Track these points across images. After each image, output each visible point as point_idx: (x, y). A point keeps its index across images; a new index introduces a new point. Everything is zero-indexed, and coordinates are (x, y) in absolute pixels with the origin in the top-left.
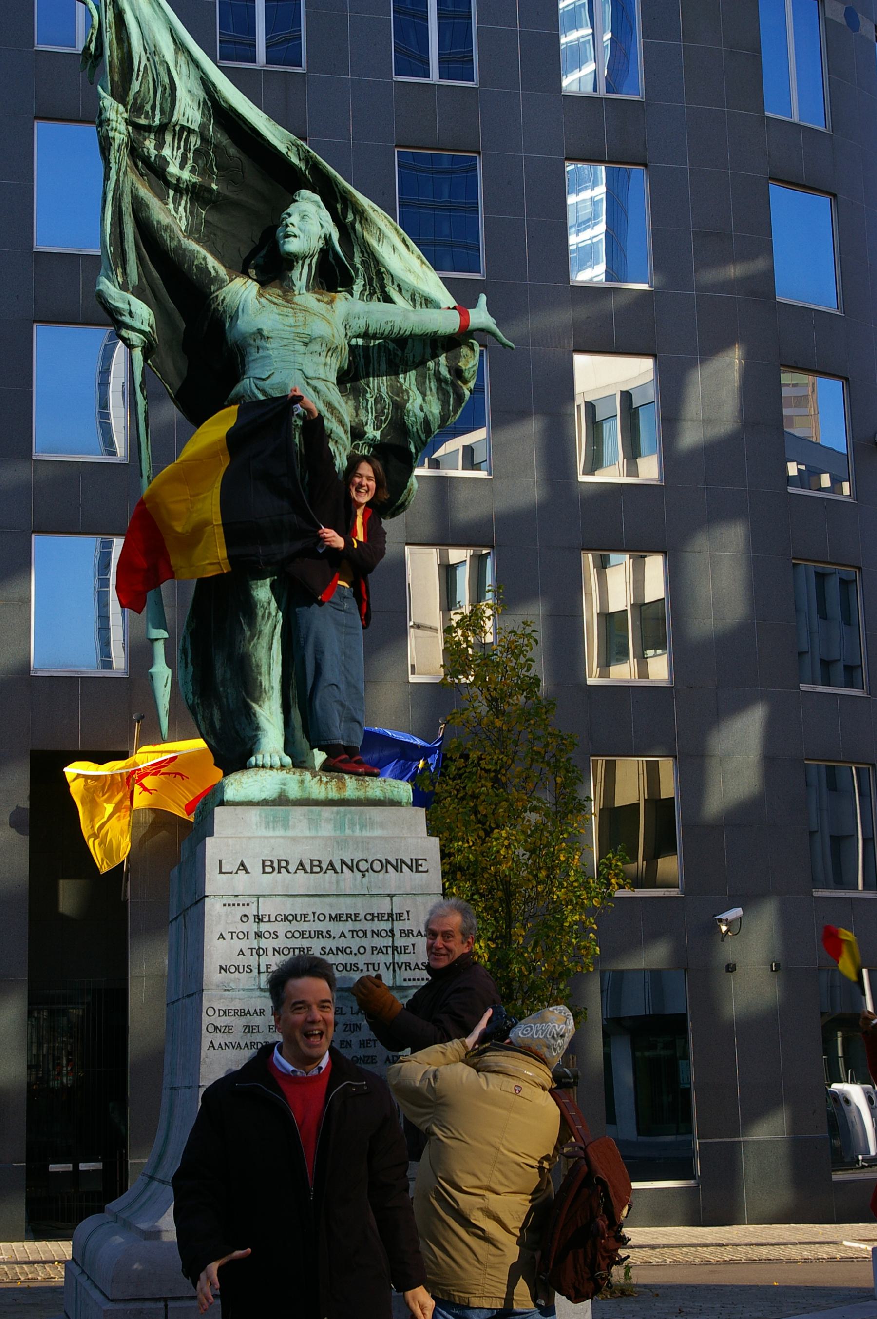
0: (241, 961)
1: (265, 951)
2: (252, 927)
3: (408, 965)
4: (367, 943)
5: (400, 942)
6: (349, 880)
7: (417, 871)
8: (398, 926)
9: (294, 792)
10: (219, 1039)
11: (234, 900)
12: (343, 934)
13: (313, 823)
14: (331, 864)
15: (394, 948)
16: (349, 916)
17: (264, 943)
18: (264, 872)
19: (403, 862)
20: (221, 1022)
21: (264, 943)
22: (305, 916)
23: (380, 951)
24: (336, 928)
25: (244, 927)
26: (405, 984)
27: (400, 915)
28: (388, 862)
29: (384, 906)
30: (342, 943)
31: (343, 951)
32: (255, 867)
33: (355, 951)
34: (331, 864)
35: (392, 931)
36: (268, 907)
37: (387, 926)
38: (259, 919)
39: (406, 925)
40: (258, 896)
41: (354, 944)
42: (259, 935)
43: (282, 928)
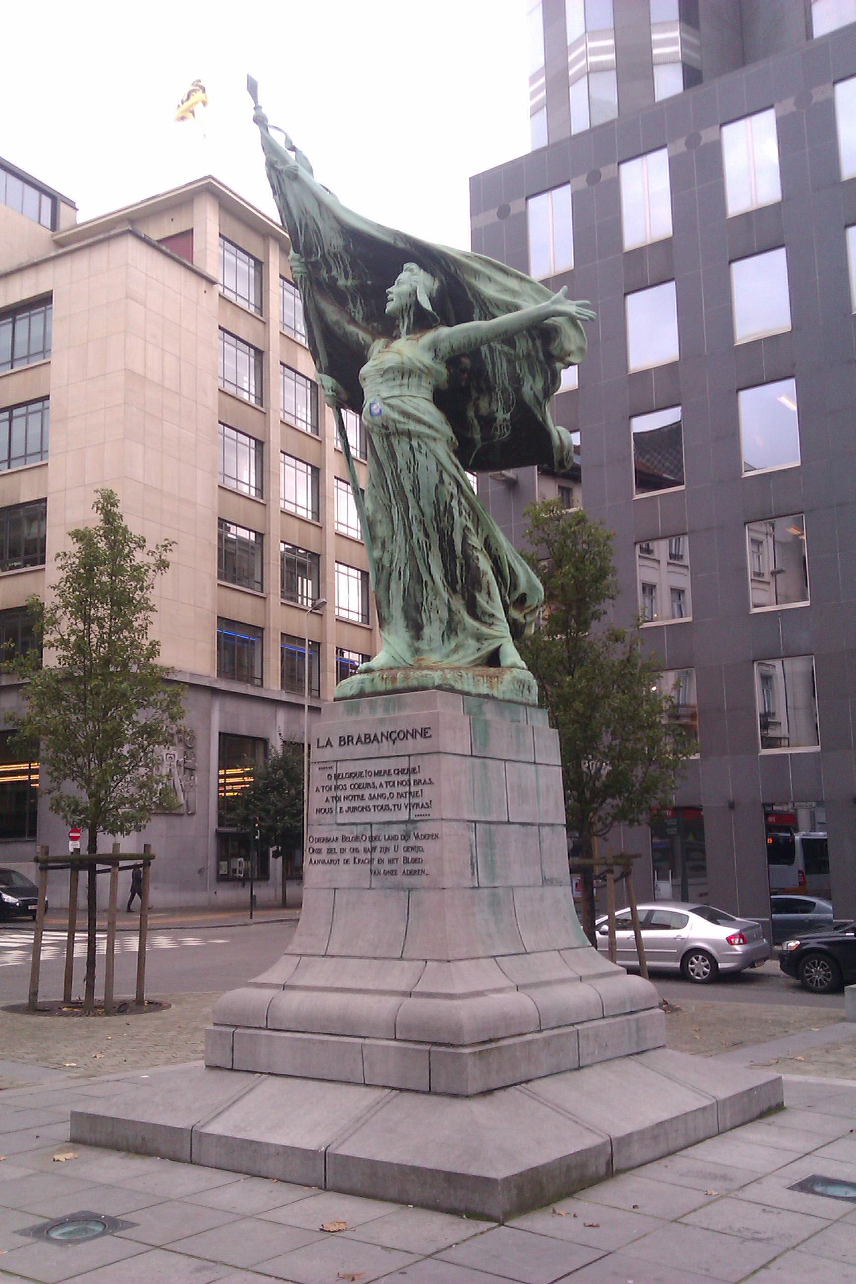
0: (327, 806)
1: (340, 799)
2: (333, 783)
3: (418, 805)
4: (395, 790)
5: (414, 789)
6: (386, 747)
7: (425, 737)
8: (413, 777)
9: (368, 688)
10: (315, 857)
11: (325, 766)
12: (381, 785)
13: (372, 708)
14: (375, 736)
15: (410, 793)
16: (385, 772)
17: (339, 793)
18: (340, 745)
19: (416, 731)
20: (316, 846)
21: (339, 793)
22: (361, 773)
23: (402, 796)
24: (378, 780)
25: (328, 783)
26: (416, 819)
27: (414, 769)
28: (408, 732)
29: (403, 763)
30: (380, 791)
31: (381, 796)
32: (335, 742)
33: (388, 795)
34: (375, 736)
35: (409, 781)
36: (343, 768)
37: (406, 777)
38: (337, 777)
39: (418, 777)
40: (337, 761)
41: (387, 791)
42: (337, 787)
43: (348, 782)
